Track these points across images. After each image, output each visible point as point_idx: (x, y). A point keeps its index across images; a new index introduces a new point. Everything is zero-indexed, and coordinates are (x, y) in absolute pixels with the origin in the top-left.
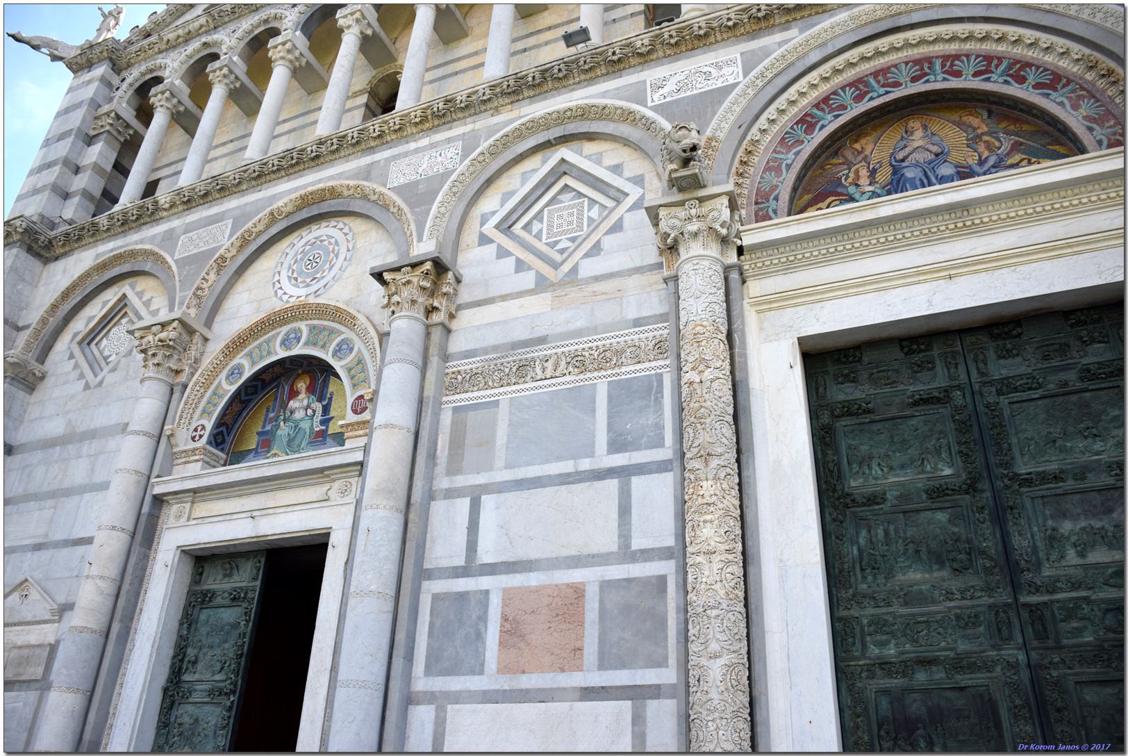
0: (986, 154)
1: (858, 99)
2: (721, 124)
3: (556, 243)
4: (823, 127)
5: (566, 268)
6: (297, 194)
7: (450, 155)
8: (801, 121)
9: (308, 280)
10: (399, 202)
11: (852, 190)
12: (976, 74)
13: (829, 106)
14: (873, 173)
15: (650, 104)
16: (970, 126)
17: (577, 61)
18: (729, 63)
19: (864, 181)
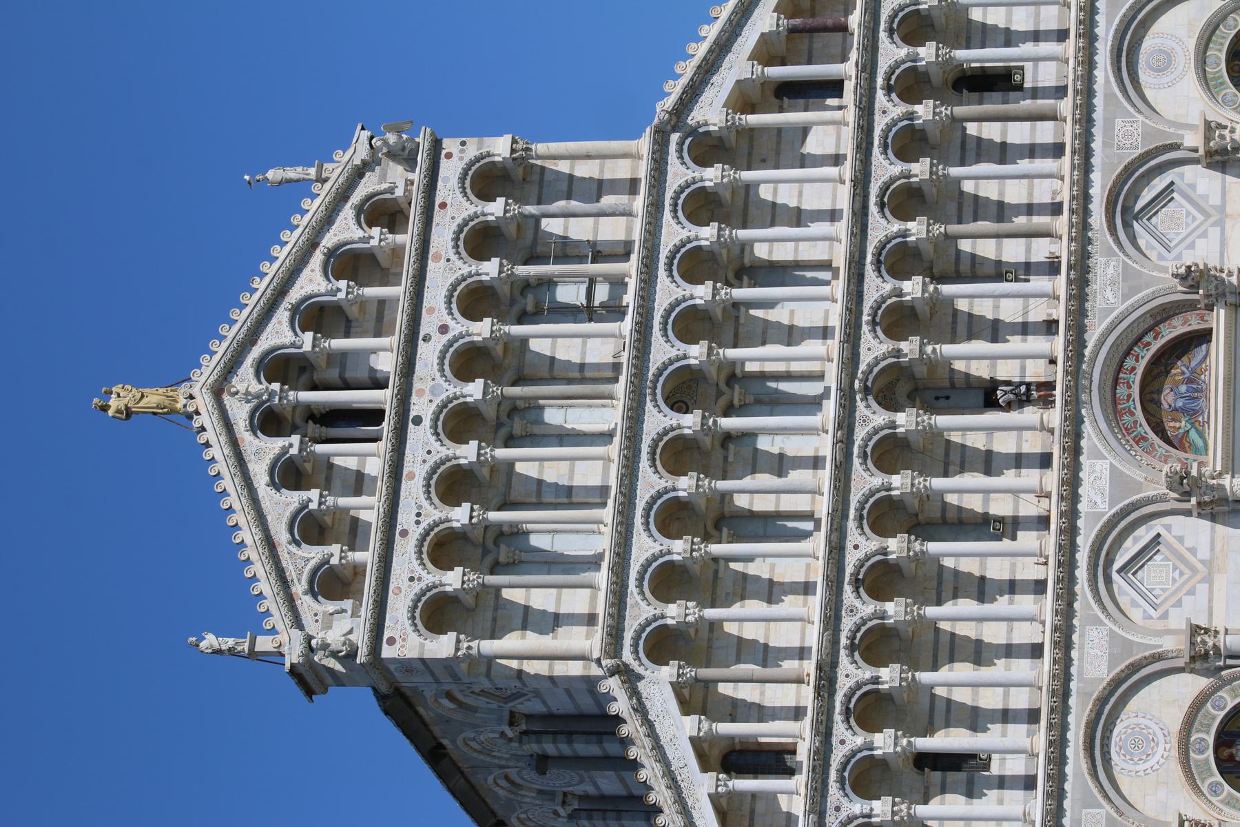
0: (1179, 370)
1: (1132, 414)
2: (1137, 475)
3: (1174, 580)
4: (1145, 433)
5: (1200, 566)
6: (1082, 753)
7: (1096, 634)
8: (1137, 443)
9: (1153, 744)
10: (1118, 669)
11: (1181, 431)
12: (1137, 360)
13: (1132, 428)
14: (1173, 420)
15: (1107, 510)
16: (1158, 374)
17: (1060, 545)
18: (1092, 466)
19: (1177, 425)
